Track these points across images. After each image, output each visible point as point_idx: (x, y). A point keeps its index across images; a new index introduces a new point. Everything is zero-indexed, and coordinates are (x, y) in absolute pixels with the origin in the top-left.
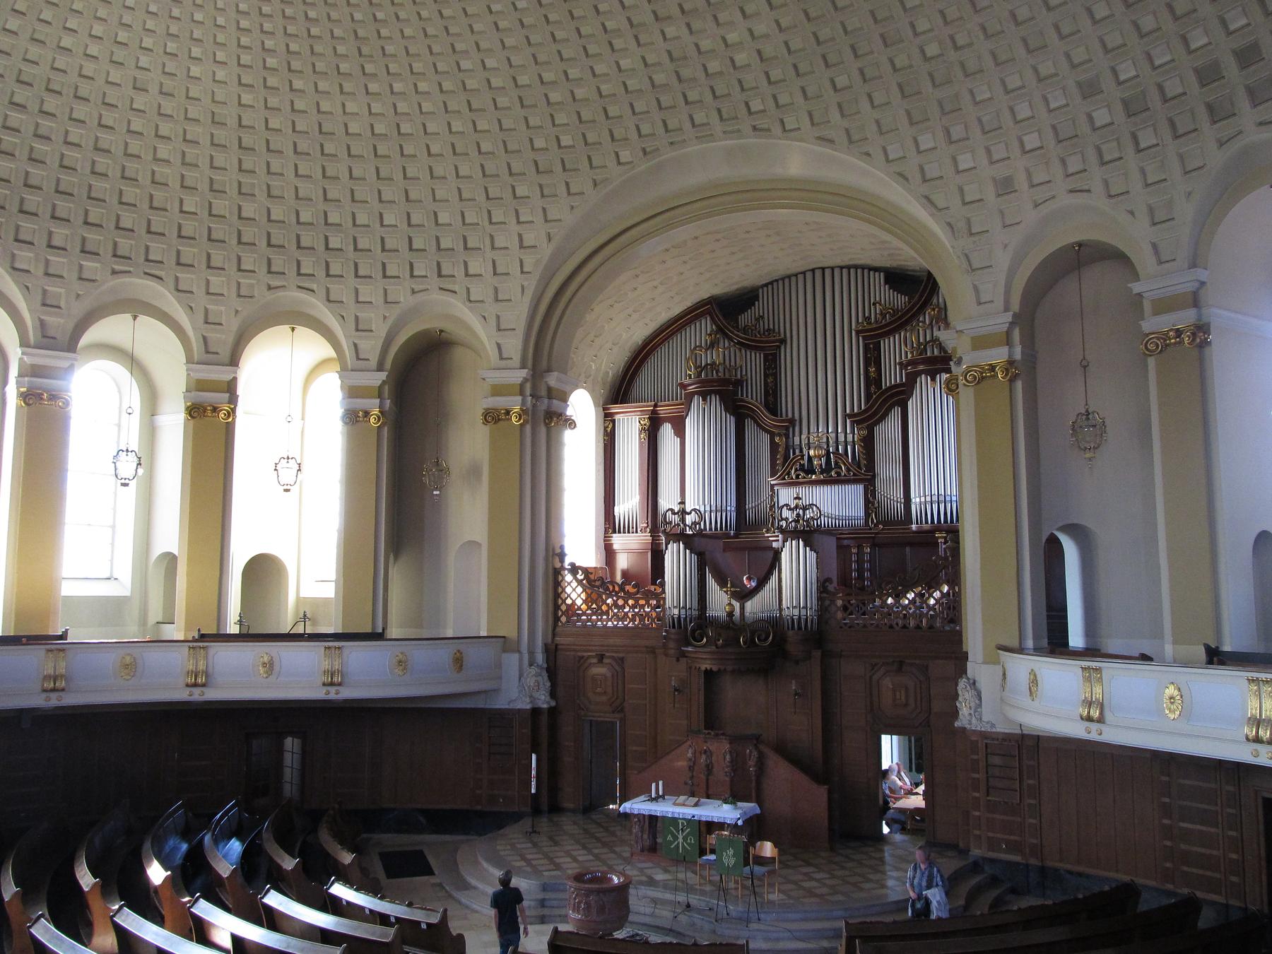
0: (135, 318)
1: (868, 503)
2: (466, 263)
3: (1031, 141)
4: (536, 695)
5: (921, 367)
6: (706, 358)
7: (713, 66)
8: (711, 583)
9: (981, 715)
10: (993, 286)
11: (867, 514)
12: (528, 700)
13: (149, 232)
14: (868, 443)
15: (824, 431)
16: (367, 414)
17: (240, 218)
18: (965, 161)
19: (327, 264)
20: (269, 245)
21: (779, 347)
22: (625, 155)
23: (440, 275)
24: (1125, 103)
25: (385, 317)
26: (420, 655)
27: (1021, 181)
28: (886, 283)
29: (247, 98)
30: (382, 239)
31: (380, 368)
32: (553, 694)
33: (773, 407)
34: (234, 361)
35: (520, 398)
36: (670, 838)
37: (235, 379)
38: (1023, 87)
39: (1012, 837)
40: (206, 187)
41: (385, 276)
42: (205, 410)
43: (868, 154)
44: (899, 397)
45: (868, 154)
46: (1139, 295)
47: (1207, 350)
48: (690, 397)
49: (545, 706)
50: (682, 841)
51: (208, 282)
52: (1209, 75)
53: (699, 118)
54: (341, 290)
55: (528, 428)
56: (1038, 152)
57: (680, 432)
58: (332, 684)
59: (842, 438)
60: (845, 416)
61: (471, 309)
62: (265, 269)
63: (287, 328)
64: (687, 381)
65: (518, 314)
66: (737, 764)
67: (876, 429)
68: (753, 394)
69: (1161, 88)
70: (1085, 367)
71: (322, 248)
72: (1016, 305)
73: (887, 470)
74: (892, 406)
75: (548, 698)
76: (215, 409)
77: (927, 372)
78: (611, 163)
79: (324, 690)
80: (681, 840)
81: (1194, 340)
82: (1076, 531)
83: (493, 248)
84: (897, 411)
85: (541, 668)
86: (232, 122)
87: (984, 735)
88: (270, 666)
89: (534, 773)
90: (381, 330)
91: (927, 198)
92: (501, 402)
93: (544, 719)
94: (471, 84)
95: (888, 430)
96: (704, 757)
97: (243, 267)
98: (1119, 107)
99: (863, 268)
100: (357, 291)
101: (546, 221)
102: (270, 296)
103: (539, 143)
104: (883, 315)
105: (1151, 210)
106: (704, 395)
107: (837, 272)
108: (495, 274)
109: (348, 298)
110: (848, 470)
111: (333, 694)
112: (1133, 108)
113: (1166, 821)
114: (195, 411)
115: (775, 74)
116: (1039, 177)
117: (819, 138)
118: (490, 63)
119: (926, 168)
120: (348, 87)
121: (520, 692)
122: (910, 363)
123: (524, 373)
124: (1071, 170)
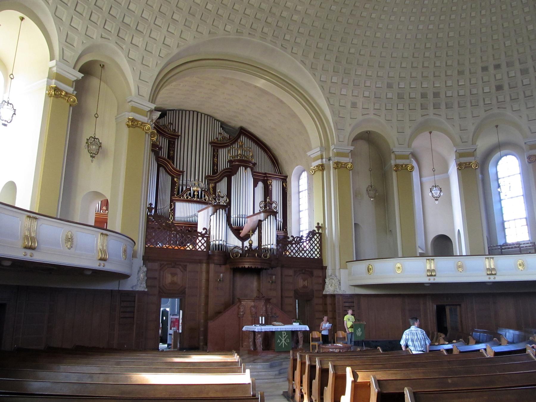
5: (237, 163)
21: (175, 139)
27: (360, 105)
28: (221, 127)
43: (314, 74)
44: (230, 172)
45: (314, 74)
50: (283, 341)
52: (424, 96)
61: (128, 62)
67: (217, 184)
77: (243, 166)
78: (221, 27)
80: (283, 341)
84: (225, 180)
87: (341, 295)
95: (222, 187)
99: (213, 117)
112: (400, 97)
117: (302, 61)
122: (235, 161)
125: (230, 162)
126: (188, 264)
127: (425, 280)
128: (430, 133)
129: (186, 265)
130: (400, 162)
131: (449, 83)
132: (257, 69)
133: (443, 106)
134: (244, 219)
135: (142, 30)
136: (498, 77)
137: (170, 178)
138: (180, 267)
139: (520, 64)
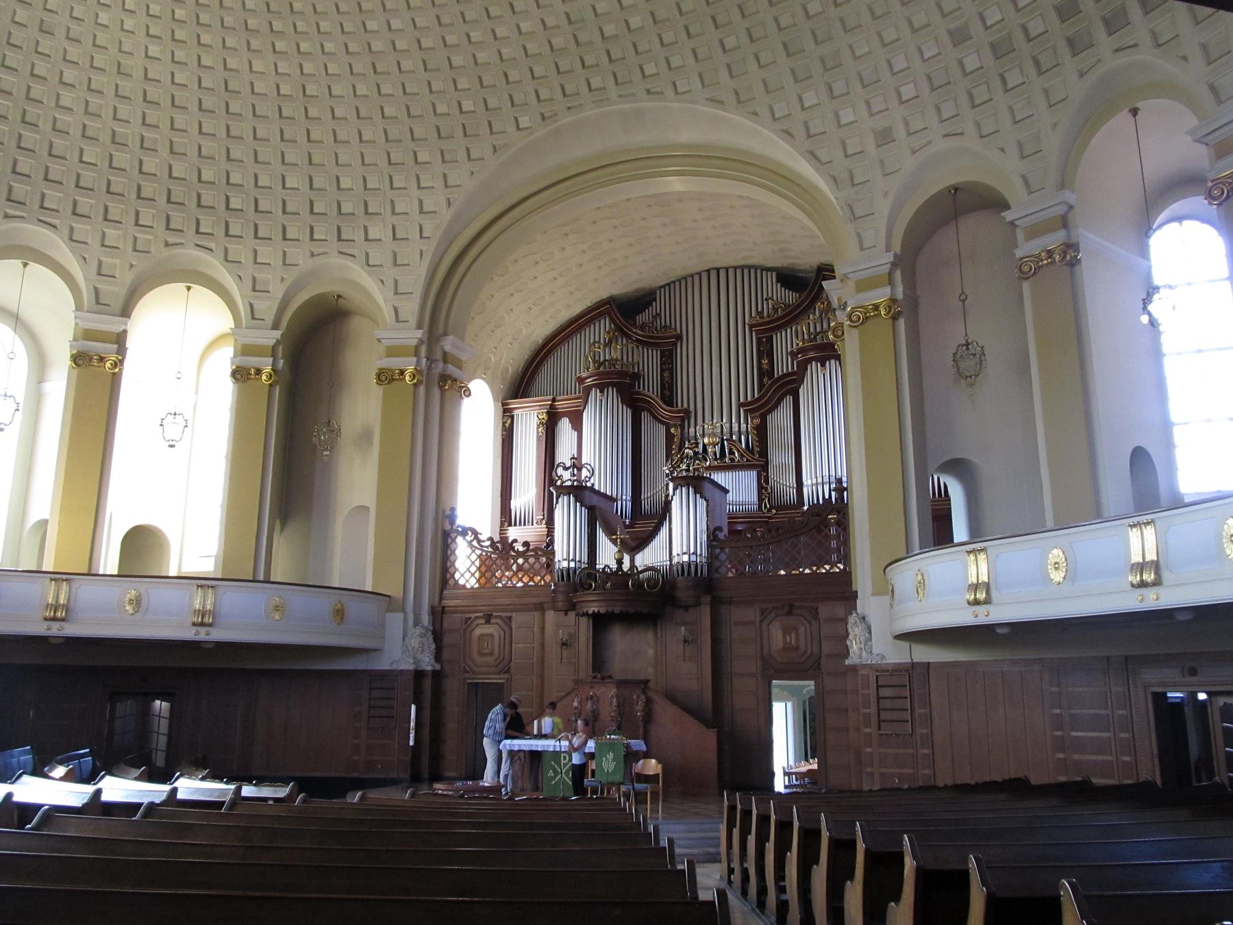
0: (25, 265)
1: (761, 488)
2: (366, 228)
3: (908, 91)
4: (420, 656)
5: (812, 355)
6: (605, 355)
7: (609, 30)
8: (603, 541)
9: (871, 648)
10: (875, 233)
11: (760, 500)
12: (411, 661)
13: (46, 179)
14: (762, 431)
15: (717, 424)
16: (259, 372)
17: (141, 172)
18: (847, 116)
19: (227, 224)
20: (169, 201)
21: (675, 344)
22: (524, 121)
23: (339, 239)
24: (993, 46)
25: (283, 279)
26: (300, 601)
27: (900, 132)
28: (778, 281)
29: (154, 50)
30: (284, 202)
31: (275, 326)
32: (438, 657)
33: (668, 396)
34: (126, 312)
35: (414, 359)
36: (551, 773)
37: (125, 332)
39: (905, 771)
40: (108, 139)
41: (284, 239)
42: (91, 359)
43: (756, 114)
45: (756, 114)
46: (1012, 223)
47: (1077, 267)
48: (587, 391)
49: (429, 668)
51: (104, 234)
53: (596, 83)
54: (240, 251)
55: (422, 389)
57: (577, 425)
58: (202, 624)
59: (735, 428)
60: (740, 405)
61: (368, 273)
62: (164, 224)
63: (182, 286)
64: (584, 375)
65: (415, 278)
66: (623, 707)
68: (650, 388)
69: (1025, 29)
70: (964, 301)
71: (223, 207)
72: (897, 247)
73: (780, 457)
74: (784, 395)
75: (433, 661)
76: (102, 359)
77: (816, 359)
78: (511, 129)
79: (194, 630)
81: (1064, 258)
82: (957, 467)
83: (393, 213)
84: (789, 399)
85: (427, 629)
86: (138, 74)
87: (870, 666)
88: (137, 602)
89: (412, 724)
90: (278, 291)
91: (812, 153)
92: (395, 363)
93: (427, 684)
94: (377, 46)
95: (781, 419)
96: (589, 705)
97: (141, 222)
98: (987, 51)
99: (756, 268)
100: (256, 252)
101: (446, 186)
102: (167, 253)
103: (442, 108)
104: (775, 310)
105: (1020, 146)
106: (602, 388)
107: (731, 272)
108: (394, 239)
109: (246, 258)
110: (742, 456)
111: (202, 635)
112: (1000, 50)
113: (1059, 733)
114: (80, 359)
115: (668, 37)
116: (916, 125)
118: (396, 24)
119: (810, 124)
120: (255, 44)
121: (403, 652)
122: (802, 350)
123: (419, 334)
124: (945, 116)
125: (794, 355)
126: (514, 614)
128: (1134, 112)
129: (510, 618)
132: (648, 162)
134: (820, 488)
135: (378, 211)
137: (663, 429)
138: (499, 621)
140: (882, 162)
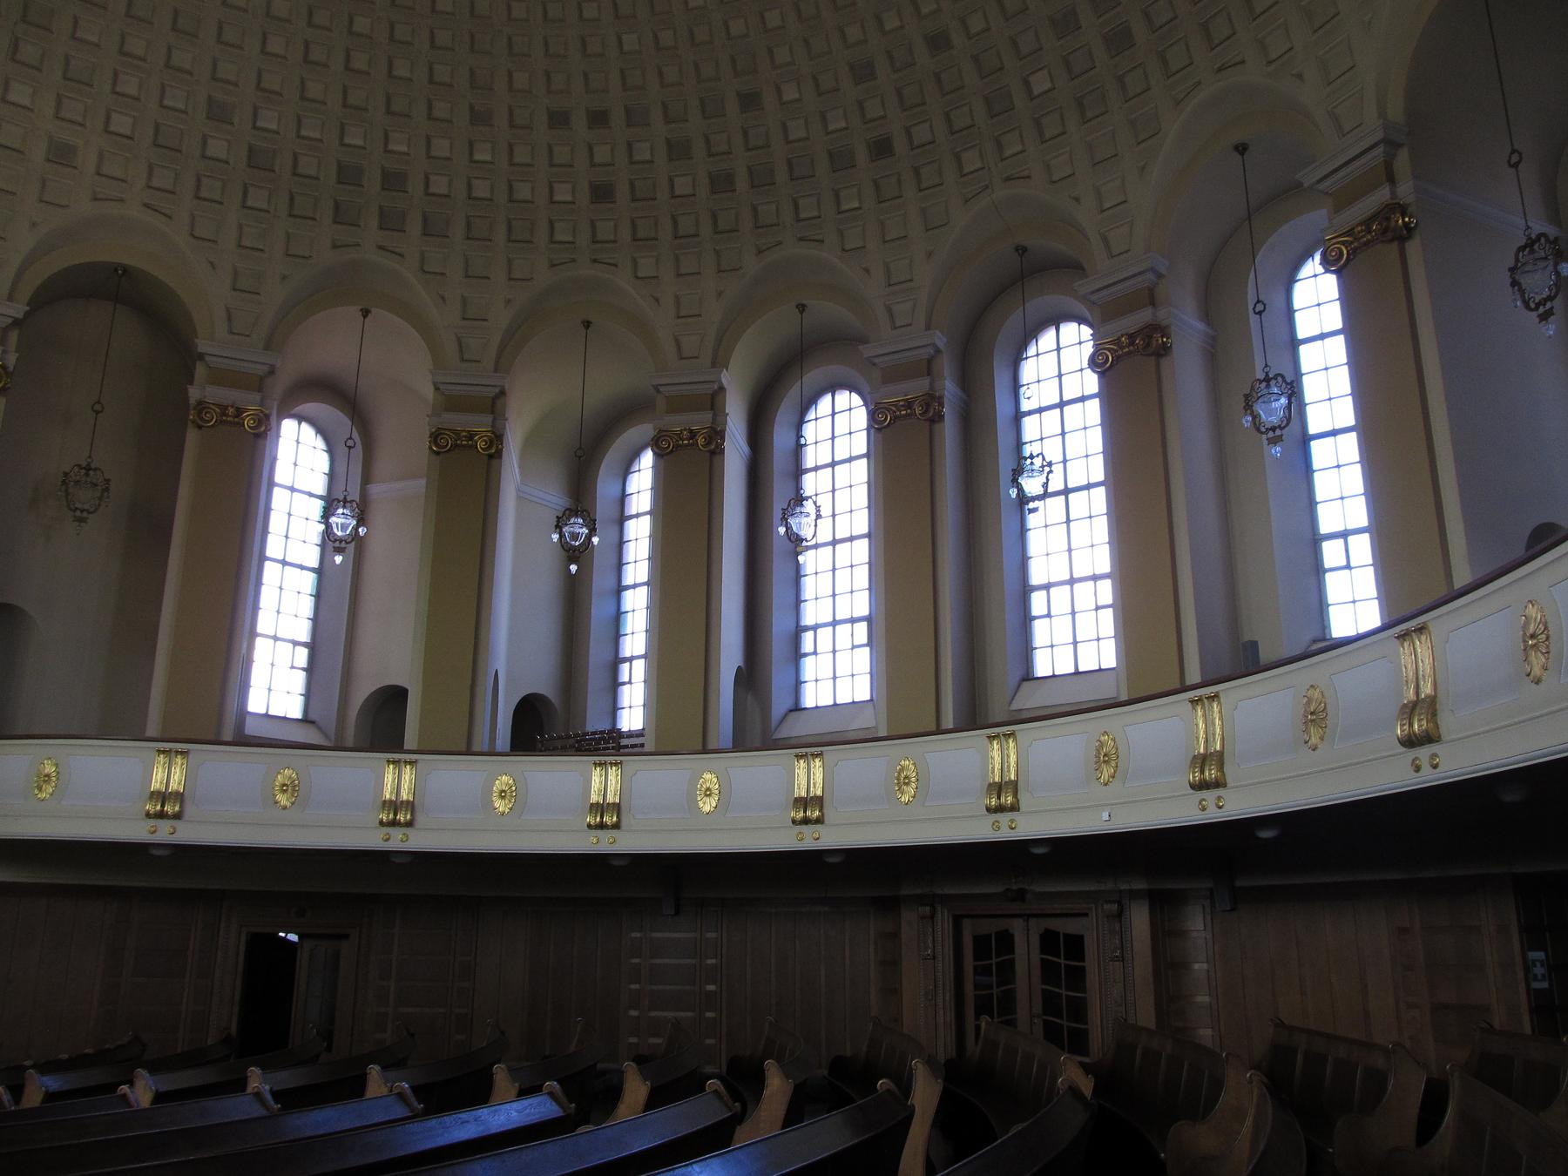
3: (121, 123)
38: (143, 60)
52: (348, 175)
56: (125, 141)
70: (97, 412)
105: (236, 274)
112: (258, 161)
127: (135, 831)
128: (366, 313)
130: (217, 394)
131: (441, 147)
133: (414, 227)
136: (602, 154)
139: (668, 120)
140: (44, 182)
